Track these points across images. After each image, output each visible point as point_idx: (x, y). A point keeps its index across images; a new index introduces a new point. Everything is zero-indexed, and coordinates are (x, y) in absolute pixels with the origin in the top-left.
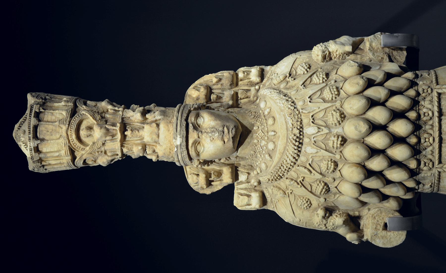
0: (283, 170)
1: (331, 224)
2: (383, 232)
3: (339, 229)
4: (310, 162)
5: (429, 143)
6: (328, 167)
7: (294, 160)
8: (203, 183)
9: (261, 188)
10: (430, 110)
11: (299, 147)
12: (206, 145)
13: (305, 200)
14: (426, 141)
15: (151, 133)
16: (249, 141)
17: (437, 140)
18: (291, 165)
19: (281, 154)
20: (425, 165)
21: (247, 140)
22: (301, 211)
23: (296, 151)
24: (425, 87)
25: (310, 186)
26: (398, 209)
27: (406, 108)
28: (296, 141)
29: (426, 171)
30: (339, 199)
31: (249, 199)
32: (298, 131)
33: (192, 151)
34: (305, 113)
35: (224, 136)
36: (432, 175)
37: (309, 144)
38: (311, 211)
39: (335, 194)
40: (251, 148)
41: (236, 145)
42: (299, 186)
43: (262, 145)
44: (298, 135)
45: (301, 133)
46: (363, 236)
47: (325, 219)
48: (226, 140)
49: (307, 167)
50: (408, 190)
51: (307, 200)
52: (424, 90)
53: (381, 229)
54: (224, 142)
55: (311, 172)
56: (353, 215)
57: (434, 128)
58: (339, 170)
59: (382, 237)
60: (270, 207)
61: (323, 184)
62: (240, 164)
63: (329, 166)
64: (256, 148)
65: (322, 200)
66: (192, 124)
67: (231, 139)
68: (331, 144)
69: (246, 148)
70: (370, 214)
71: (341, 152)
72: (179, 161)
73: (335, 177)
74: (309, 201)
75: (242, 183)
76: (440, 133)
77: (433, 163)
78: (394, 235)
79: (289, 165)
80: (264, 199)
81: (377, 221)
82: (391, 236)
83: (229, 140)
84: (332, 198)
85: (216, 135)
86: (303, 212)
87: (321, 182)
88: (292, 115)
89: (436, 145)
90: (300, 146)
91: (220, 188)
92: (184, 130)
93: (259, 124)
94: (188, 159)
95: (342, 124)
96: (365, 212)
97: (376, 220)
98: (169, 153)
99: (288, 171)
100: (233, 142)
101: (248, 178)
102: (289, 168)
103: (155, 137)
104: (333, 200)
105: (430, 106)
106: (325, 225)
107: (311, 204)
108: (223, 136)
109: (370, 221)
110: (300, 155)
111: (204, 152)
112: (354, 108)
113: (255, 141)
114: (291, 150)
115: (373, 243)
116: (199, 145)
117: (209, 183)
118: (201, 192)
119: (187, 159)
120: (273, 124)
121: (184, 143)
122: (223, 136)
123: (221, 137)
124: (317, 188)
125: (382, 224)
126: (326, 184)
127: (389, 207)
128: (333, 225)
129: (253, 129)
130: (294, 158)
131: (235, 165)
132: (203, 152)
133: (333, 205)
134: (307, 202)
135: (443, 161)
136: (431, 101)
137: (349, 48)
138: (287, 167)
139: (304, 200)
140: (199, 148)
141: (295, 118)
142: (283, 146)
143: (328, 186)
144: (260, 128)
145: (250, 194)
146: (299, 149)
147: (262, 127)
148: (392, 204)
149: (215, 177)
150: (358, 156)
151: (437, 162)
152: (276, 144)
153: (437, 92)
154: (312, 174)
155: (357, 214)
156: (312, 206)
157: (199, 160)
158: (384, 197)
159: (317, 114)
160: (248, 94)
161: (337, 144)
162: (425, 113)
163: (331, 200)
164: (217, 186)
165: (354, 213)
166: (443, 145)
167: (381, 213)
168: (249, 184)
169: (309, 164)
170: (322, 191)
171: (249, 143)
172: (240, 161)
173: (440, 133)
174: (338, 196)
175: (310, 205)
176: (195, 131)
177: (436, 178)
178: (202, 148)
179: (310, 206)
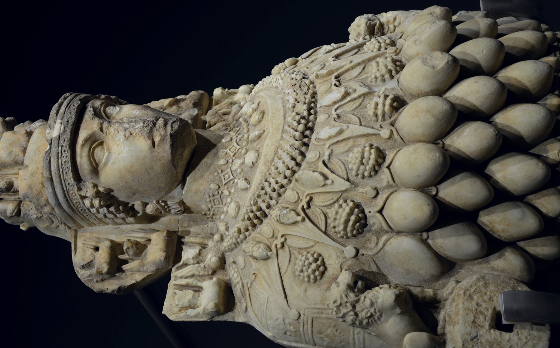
0: (269, 190)
1: (368, 302)
2: (492, 331)
3: (386, 321)
4: (326, 158)
6: (363, 157)
7: (292, 164)
8: (103, 261)
9: (226, 275)
11: (306, 137)
12: (115, 149)
13: (313, 255)
15: (11, 144)
16: (209, 161)
18: (286, 177)
19: (268, 164)
21: (205, 160)
22: (303, 288)
23: (297, 143)
25: (323, 218)
27: (533, 47)
28: (299, 123)
30: (387, 248)
31: (197, 294)
32: (305, 107)
33: (81, 157)
34: (323, 76)
35: (155, 130)
37: (326, 123)
38: (325, 286)
39: (379, 233)
40: (211, 177)
41: (181, 170)
42: (299, 219)
43: (234, 168)
44: (305, 114)
45: (312, 111)
47: (354, 292)
48: (157, 139)
49: (319, 170)
51: (315, 256)
53: (487, 325)
54: (154, 143)
55: (326, 178)
58: (388, 167)
60: (238, 316)
61: (351, 204)
62: (188, 233)
63: (366, 155)
64: (222, 175)
65: (349, 251)
66: (95, 109)
67: (168, 138)
68: (371, 112)
69: (202, 177)
70: (460, 288)
71: (392, 124)
72: (51, 180)
73: (378, 186)
74: (320, 259)
75: (185, 265)
78: (519, 339)
79: (282, 176)
80: (227, 297)
81: (478, 304)
83: (163, 140)
84: (372, 245)
85: (138, 126)
86: (306, 290)
87: (348, 201)
88: (298, 85)
90: (308, 133)
91: (138, 277)
92: (74, 112)
93: (234, 134)
94: (70, 175)
95: (396, 77)
97: (474, 303)
98: (40, 185)
99: (279, 195)
100: (173, 146)
101: (199, 254)
102: (282, 186)
103: (17, 150)
104: (375, 251)
106: (354, 307)
107: (326, 269)
108: (151, 129)
109: (461, 305)
110: (307, 154)
111: (110, 164)
112: (423, 38)
113: (222, 162)
114: (290, 143)
116: (100, 147)
117: (116, 265)
118: (97, 287)
119: (69, 177)
120: (260, 121)
121: (68, 135)
122: (151, 129)
123: (147, 130)
124: (337, 213)
125: (489, 313)
126: (357, 206)
127: (503, 271)
128: (372, 304)
129: (220, 141)
130: (293, 159)
131: (179, 234)
132: (106, 163)
133: (374, 269)
134: (316, 260)
138: (277, 183)
139: (309, 255)
140: (98, 153)
141: (301, 90)
142: (273, 147)
143: (363, 211)
144: (234, 140)
145: (199, 284)
146: (306, 140)
147: (239, 137)
149: (130, 245)
150: (428, 111)
152: (260, 151)
154: (329, 182)
155: (429, 292)
156: (327, 274)
157: (95, 186)
158: (492, 245)
159: (347, 74)
160: (226, 117)
161: (384, 105)
163: (370, 253)
164: (134, 274)
165: (423, 291)
167: (486, 285)
168: (202, 265)
169: (324, 162)
170: (347, 221)
171: (208, 166)
172: (189, 226)
174: (384, 238)
175: (322, 268)
176: (97, 119)
178: (106, 154)
179: (323, 274)
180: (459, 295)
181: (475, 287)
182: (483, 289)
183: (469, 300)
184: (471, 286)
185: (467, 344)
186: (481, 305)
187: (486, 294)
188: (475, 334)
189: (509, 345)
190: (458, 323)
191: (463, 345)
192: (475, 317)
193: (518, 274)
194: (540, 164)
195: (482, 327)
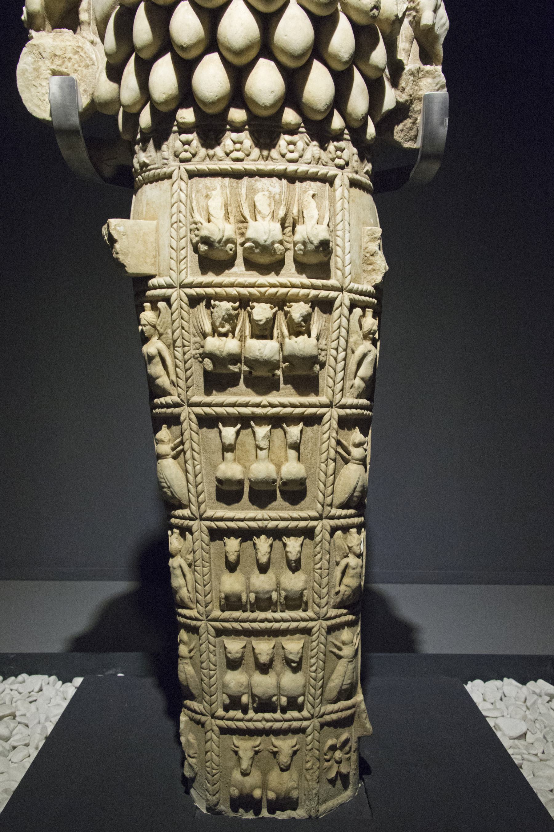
5: (232, 149)
10: (301, 156)
14: (235, 143)
17: (238, 166)
20: (184, 143)
24: (345, 155)
26: (97, 100)
29: (174, 146)
36: (165, 161)
46: (38, 30)
50: (132, 118)
52: (342, 150)
56: (81, 8)
57: (262, 162)
59: (36, 70)
70: (84, 43)
76: (251, 174)
77: (188, 160)
78: (43, 94)
81: (70, 58)
82: (39, 89)
89: (227, 165)
96: (89, 33)
97: (71, 55)
105: (308, 156)
109: (68, 43)
115: (25, 50)
127: (98, 80)
135: (195, 180)
136: (318, 161)
137: (427, 18)
148: (105, 88)
151: (190, 166)
153: (335, 176)
155: (83, 16)
162: (294, 144)
166: (227, 179)
173: (251, 174)
177: (159, 171)
180: (78, 42)
181: (84, 56)
182: (84, 64)
183: (73, 51)
184: (85, 53)
185: (36, 49)
186: (70, 62)
187: (80, 66)
188: (44, 56)
189: (37, 86)
190: (54, 41)
191: (35, 45)
192: (59, 56)
193: (96, 94)
194: (164, 96)
195: (52, 63)
